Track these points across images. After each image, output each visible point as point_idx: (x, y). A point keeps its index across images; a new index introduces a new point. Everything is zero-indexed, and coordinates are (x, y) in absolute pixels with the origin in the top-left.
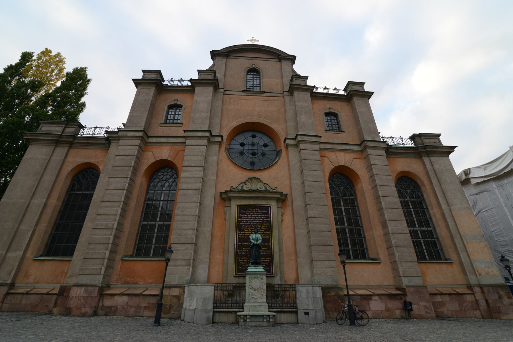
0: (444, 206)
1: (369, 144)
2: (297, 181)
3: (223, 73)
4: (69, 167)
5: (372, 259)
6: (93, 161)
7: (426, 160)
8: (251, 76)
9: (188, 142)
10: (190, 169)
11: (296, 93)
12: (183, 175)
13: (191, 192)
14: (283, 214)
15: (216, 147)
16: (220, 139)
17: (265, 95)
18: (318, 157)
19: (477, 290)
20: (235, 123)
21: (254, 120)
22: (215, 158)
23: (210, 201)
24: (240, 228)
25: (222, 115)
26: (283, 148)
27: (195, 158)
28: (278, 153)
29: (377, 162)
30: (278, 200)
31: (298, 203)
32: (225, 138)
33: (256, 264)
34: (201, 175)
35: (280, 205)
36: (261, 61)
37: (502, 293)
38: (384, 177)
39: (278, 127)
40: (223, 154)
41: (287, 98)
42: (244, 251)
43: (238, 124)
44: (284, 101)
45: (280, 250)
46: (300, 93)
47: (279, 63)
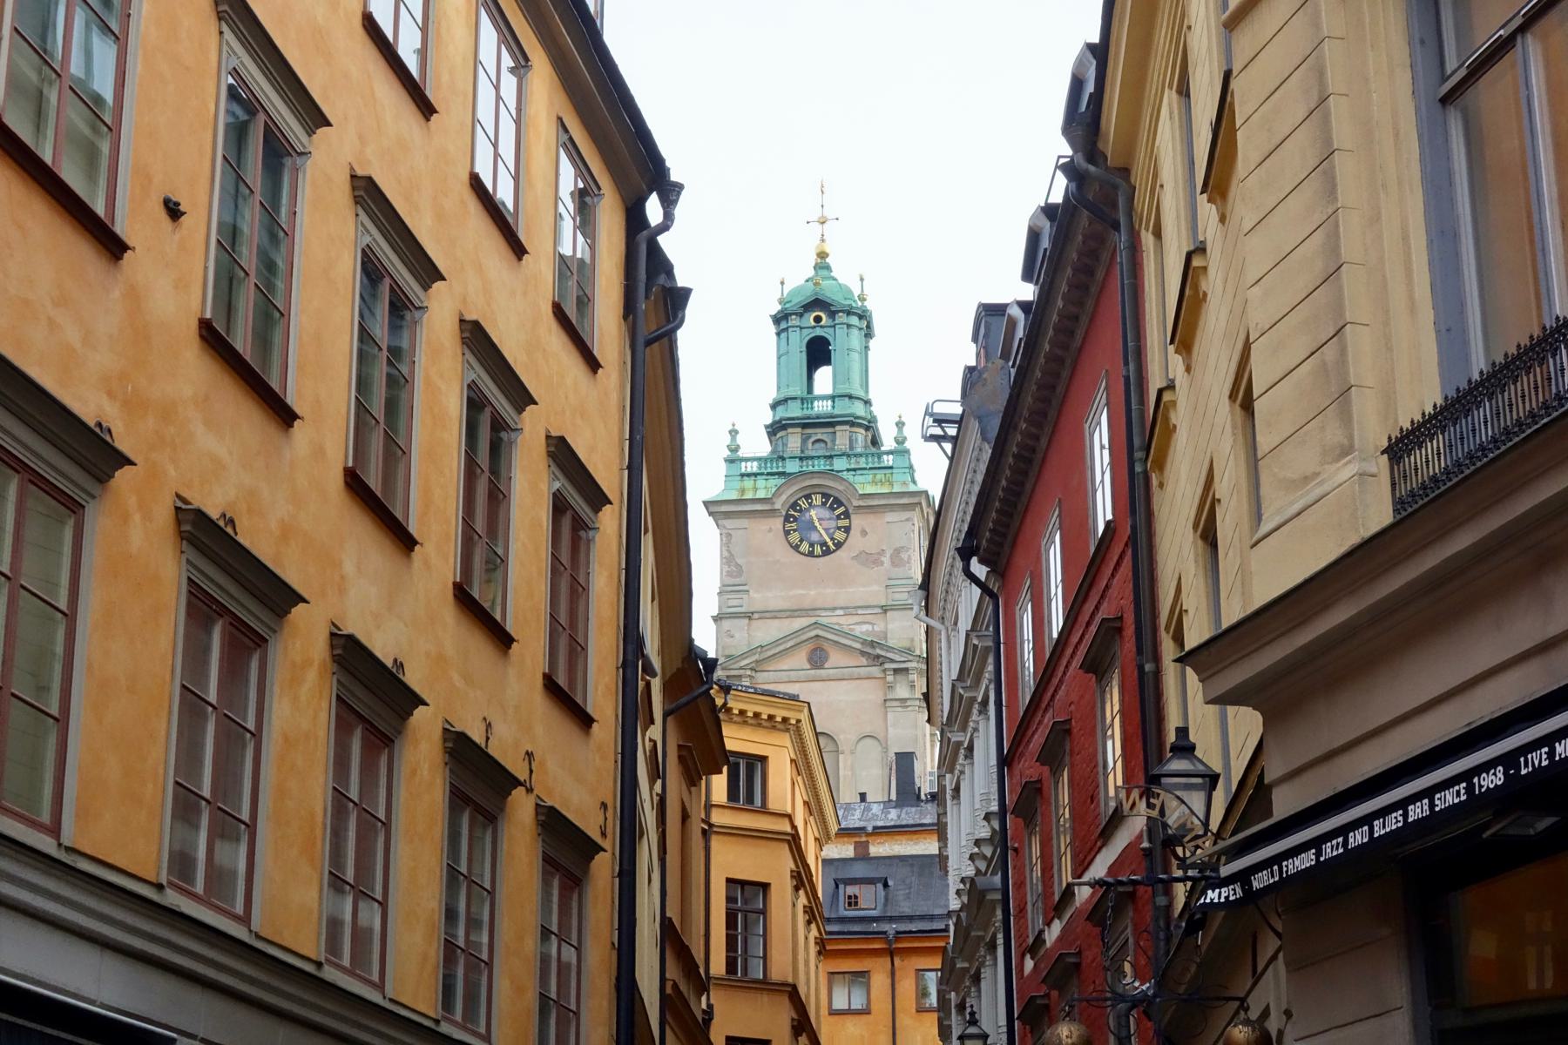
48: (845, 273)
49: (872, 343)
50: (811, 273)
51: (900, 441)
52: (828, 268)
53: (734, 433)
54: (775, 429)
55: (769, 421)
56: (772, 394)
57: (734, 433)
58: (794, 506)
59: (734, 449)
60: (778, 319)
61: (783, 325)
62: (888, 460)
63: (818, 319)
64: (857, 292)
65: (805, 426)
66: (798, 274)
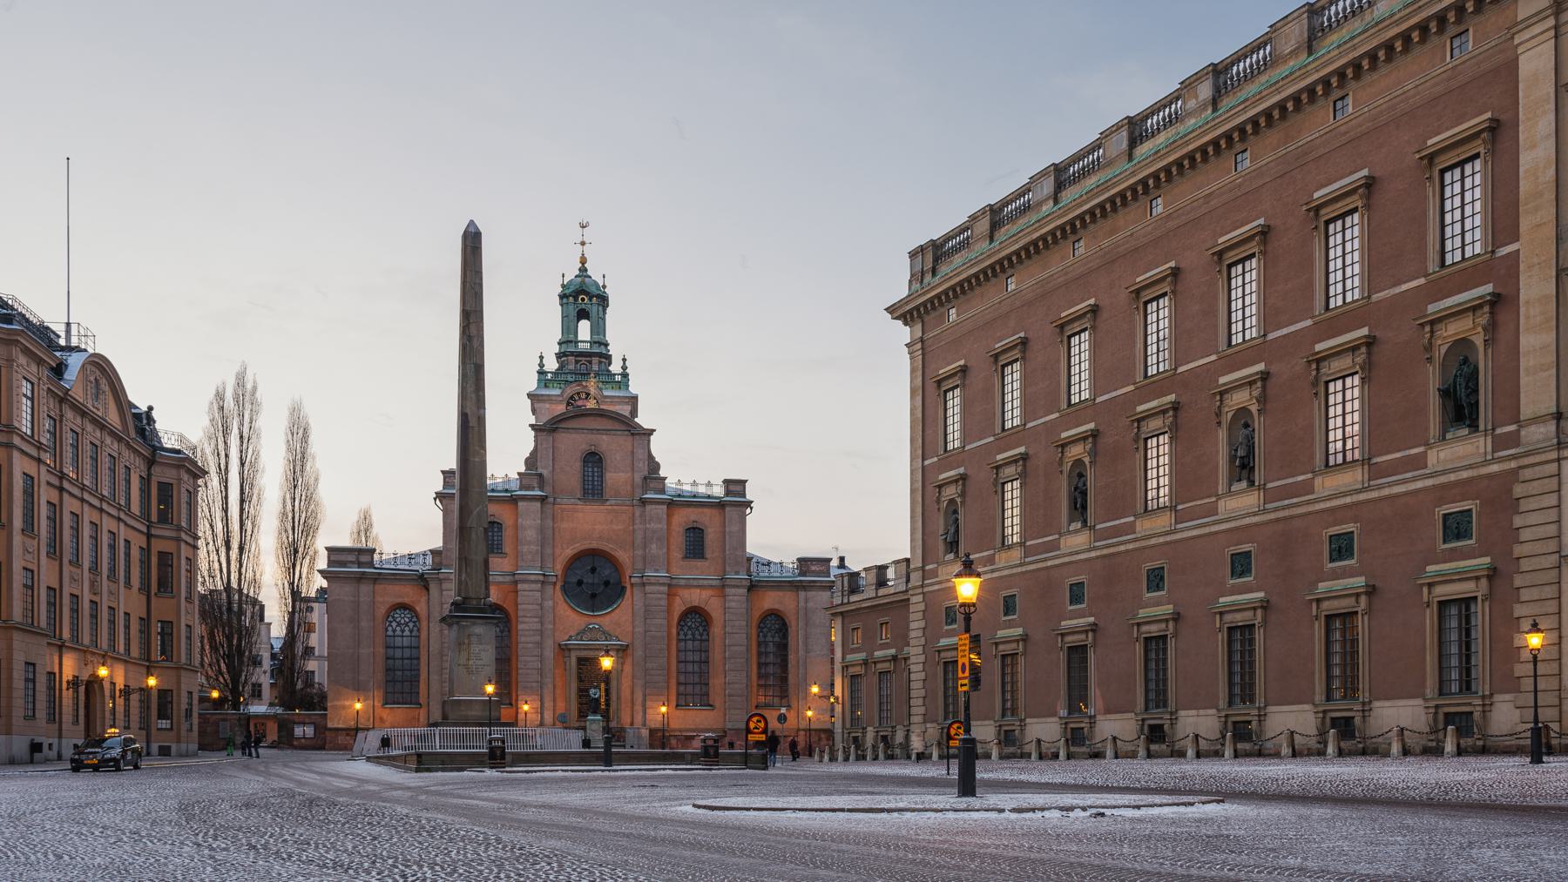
0: (801, 653)
1: (728, 582)
2: (640, 629)
3: (551, 468)
4: (382, 610)
5: (711, 706)
6: (406, 600)
7: (802, 594)
8: (590, 465)
9: (520, 586)
10: (527, 620)
11: (648, 507)
12: (520, 627)
13: (530, 645)
14: (623, 664)
15: (549, 589)
16: (554, 579)
17: (608, 503)
18: (664, 603)
19: (802, 733)
20: (569, 552)
21: (594, 545)
22: (550, 603)
23: (549, 653)
24: (580, 680)
25: (553, 539)
26: (628, 586)
27: (530, 607)
28: (624, 588)
29: (733, 604)
30: (618, 650)
31: (639, 653)
32: (559, 573)
33: (595, 712)
34: (539, 627)
35: (620, 655)
36: (604, 437)
37: (823, 736)
38: (737, 623)
39: (623, 556)
40: (559, 593)
41: (638, 512)
42: (584, 700)
43: (575, 551)
44: (633, 514)
45: (619, 698)
46: (653, 507)
47: (630, 438)
48: (595, 273)
49: (608, 310)
50: (578, 272)
51: (624, 368)
52: (586, 270)
53: (541, 358)
54: (559, 356)
55: (557, 351)
56: (559, 336)
57: (541, 358)
58: (572, 398)
59: (541, 365)
60: (562, 297)
61: (565, 300)
62: (618, 378)
63: (583, 299)
64: (601, 285)
65: (576, 356)
66: (572, 273)
